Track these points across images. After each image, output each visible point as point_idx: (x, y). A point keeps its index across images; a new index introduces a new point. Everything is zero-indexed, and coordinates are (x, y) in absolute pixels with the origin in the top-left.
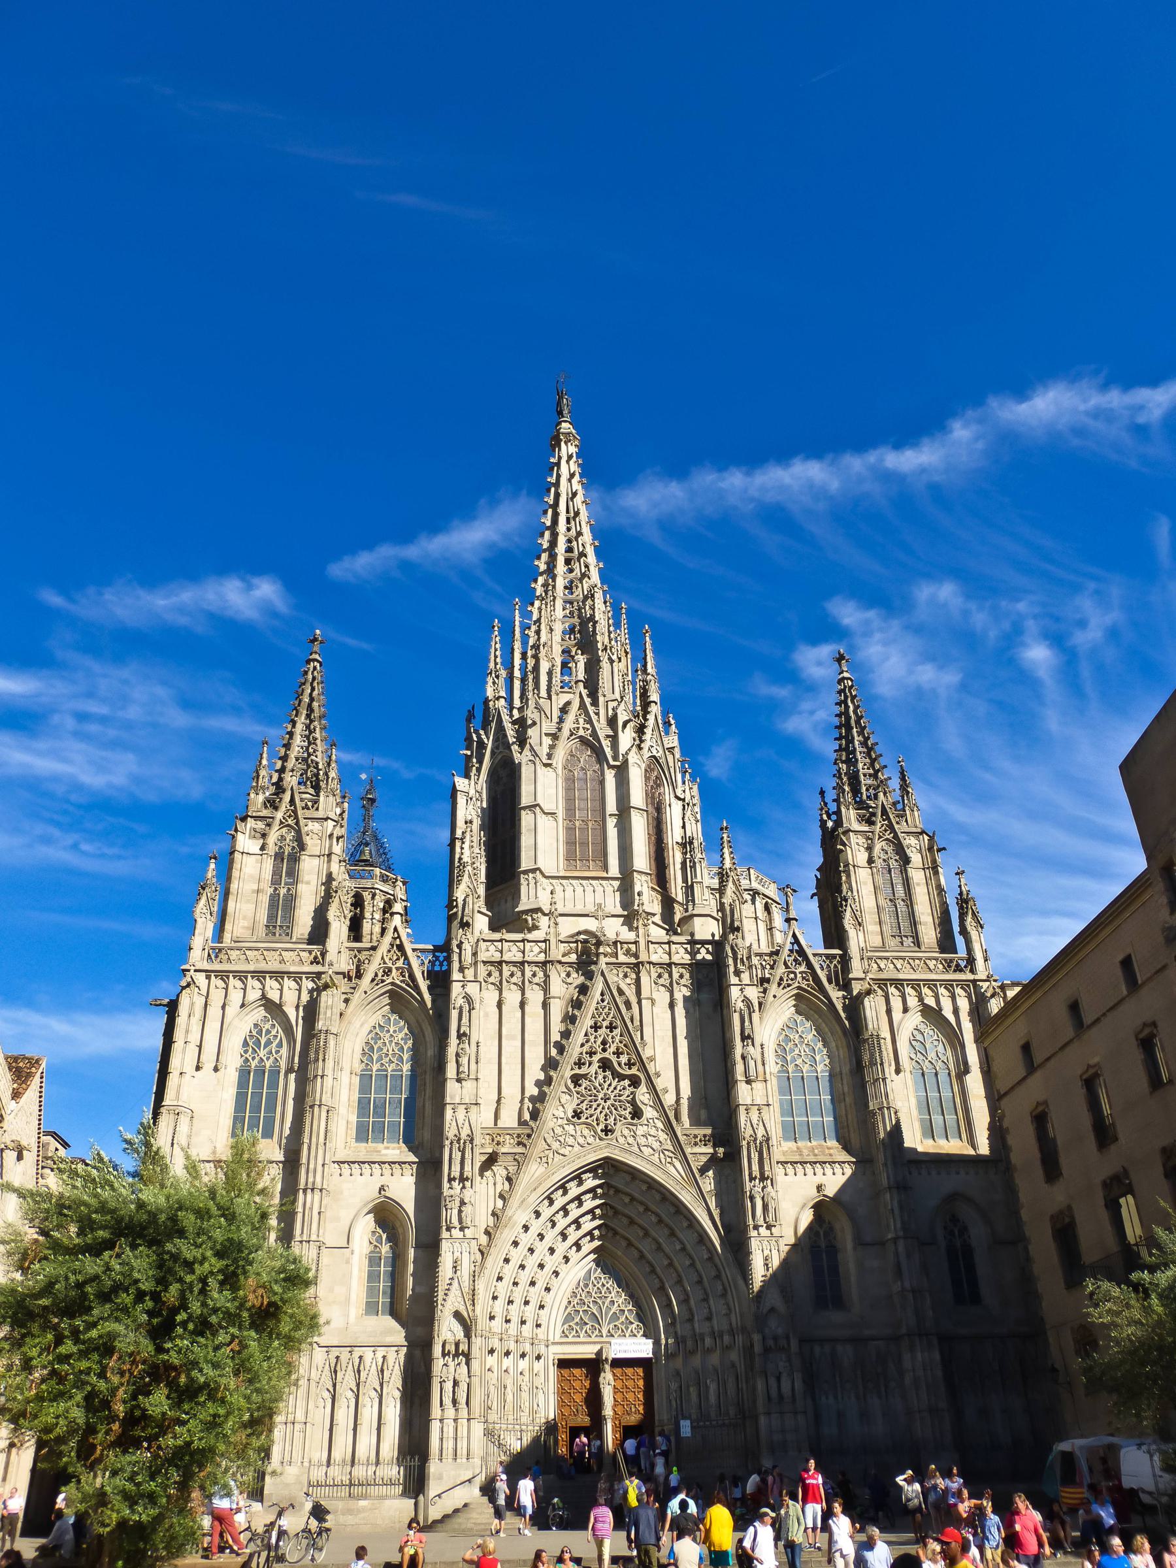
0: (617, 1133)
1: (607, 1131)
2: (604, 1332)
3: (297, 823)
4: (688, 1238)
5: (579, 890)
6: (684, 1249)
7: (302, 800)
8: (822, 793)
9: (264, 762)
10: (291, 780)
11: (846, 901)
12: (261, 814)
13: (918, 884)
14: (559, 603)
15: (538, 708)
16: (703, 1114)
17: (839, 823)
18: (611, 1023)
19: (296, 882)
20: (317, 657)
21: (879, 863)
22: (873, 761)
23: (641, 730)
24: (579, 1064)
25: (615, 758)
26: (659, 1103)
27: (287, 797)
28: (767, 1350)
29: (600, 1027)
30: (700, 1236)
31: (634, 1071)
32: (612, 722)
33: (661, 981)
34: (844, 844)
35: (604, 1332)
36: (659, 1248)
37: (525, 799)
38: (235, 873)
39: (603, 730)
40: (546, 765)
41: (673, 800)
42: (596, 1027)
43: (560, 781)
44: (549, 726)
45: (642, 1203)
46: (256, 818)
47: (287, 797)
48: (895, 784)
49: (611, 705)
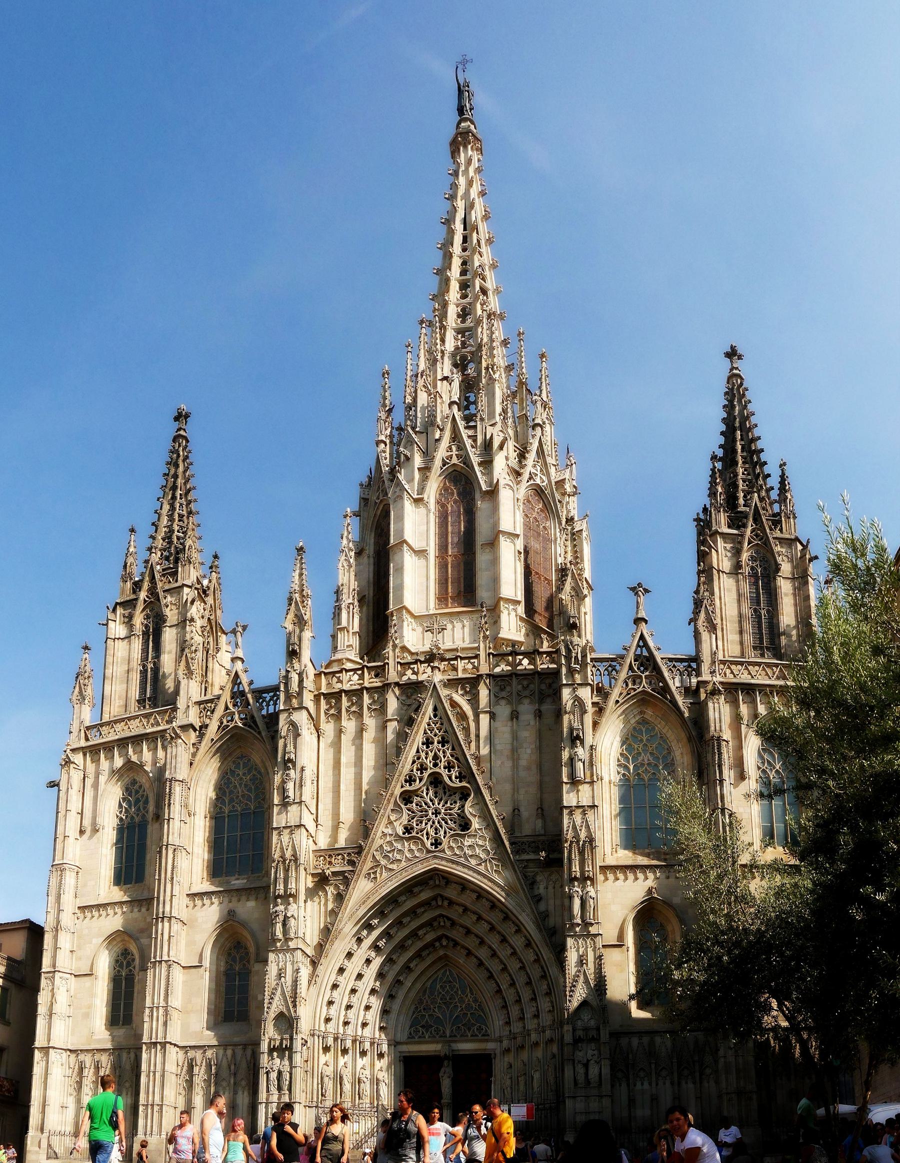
0: (445, 845)
1: (437, 843)
2: (448, 1033)
4: (518, 942)
6: (514, 953)
16: (539, 823)
18: (443, 738)
24: (410, 780)
26: (486, 815)
28: (577, 1041)
29: (432, 743)
30: (528, 940)
31: (464, 784)
32: (488, 445)
33: (504, 694)
35: (448, 1033)
36: (494, 955)
42: (428, 742)
45: (474, 913)
49: (490, 430)
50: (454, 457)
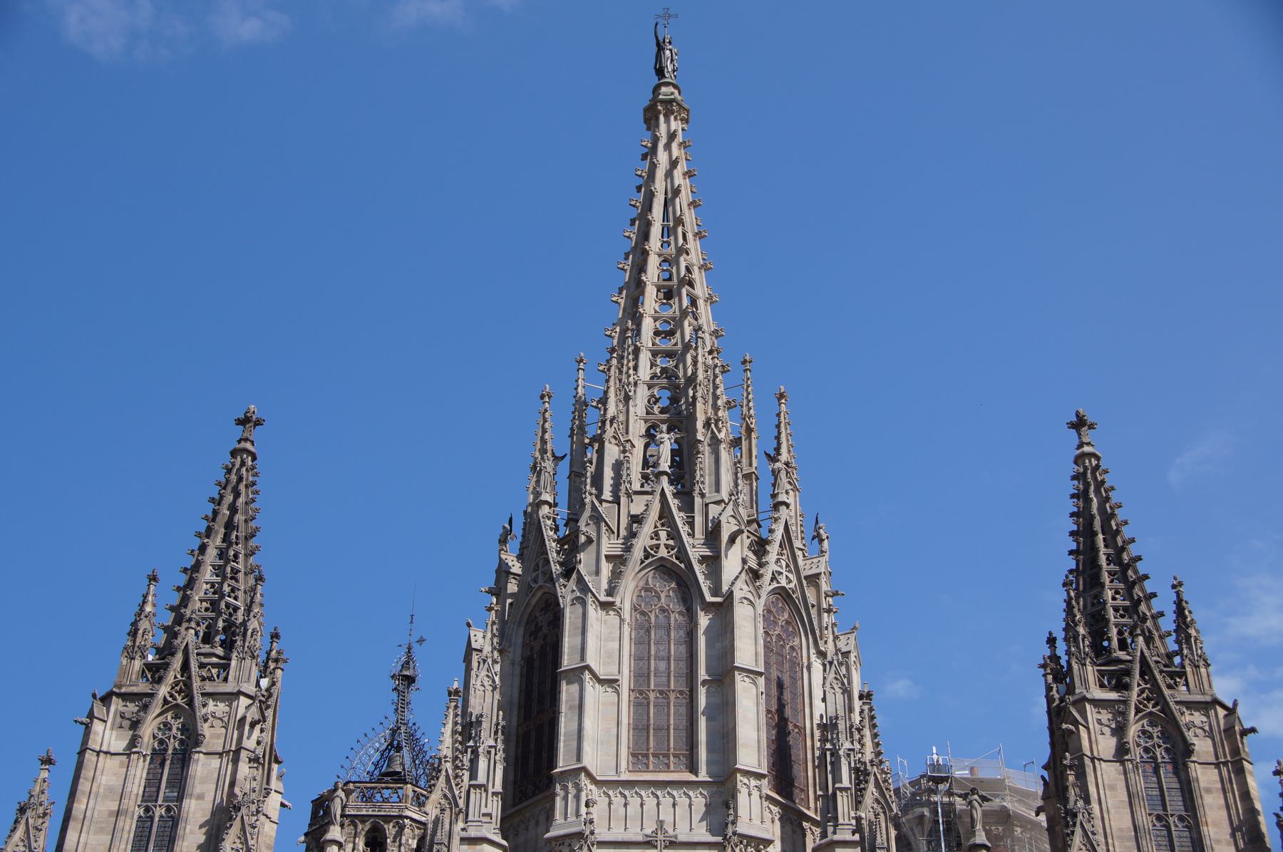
3: (191, 703)
5: (650, 802)
7: (202, 666)
8: (1051, 641)
9: (148, 608)
10: (189, 636)
11: (1075, 815)
12: (134, 689)
13: (1208, 791)
14: (645, 357)
15: (597, 518)
17: (1071, 689)
19: (180, 799)
20: (248, 446)
21: (1136, 753)
22: (1130, 586)
23: (760, 547)
25: (716, 591)
27: (177, 662)
32: (713, 535)
34: (1075, 723)
37: (568, 661)
38: (84, 786)
39: (696, 549)
40: (606, 606)
41: (813, 657)
43: (626, 629)
44: (609, 545)
46: (126, 697)
47: (177, 662)
48: (1168, 624)
49: (714, 511)
50: (662, 547)
